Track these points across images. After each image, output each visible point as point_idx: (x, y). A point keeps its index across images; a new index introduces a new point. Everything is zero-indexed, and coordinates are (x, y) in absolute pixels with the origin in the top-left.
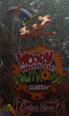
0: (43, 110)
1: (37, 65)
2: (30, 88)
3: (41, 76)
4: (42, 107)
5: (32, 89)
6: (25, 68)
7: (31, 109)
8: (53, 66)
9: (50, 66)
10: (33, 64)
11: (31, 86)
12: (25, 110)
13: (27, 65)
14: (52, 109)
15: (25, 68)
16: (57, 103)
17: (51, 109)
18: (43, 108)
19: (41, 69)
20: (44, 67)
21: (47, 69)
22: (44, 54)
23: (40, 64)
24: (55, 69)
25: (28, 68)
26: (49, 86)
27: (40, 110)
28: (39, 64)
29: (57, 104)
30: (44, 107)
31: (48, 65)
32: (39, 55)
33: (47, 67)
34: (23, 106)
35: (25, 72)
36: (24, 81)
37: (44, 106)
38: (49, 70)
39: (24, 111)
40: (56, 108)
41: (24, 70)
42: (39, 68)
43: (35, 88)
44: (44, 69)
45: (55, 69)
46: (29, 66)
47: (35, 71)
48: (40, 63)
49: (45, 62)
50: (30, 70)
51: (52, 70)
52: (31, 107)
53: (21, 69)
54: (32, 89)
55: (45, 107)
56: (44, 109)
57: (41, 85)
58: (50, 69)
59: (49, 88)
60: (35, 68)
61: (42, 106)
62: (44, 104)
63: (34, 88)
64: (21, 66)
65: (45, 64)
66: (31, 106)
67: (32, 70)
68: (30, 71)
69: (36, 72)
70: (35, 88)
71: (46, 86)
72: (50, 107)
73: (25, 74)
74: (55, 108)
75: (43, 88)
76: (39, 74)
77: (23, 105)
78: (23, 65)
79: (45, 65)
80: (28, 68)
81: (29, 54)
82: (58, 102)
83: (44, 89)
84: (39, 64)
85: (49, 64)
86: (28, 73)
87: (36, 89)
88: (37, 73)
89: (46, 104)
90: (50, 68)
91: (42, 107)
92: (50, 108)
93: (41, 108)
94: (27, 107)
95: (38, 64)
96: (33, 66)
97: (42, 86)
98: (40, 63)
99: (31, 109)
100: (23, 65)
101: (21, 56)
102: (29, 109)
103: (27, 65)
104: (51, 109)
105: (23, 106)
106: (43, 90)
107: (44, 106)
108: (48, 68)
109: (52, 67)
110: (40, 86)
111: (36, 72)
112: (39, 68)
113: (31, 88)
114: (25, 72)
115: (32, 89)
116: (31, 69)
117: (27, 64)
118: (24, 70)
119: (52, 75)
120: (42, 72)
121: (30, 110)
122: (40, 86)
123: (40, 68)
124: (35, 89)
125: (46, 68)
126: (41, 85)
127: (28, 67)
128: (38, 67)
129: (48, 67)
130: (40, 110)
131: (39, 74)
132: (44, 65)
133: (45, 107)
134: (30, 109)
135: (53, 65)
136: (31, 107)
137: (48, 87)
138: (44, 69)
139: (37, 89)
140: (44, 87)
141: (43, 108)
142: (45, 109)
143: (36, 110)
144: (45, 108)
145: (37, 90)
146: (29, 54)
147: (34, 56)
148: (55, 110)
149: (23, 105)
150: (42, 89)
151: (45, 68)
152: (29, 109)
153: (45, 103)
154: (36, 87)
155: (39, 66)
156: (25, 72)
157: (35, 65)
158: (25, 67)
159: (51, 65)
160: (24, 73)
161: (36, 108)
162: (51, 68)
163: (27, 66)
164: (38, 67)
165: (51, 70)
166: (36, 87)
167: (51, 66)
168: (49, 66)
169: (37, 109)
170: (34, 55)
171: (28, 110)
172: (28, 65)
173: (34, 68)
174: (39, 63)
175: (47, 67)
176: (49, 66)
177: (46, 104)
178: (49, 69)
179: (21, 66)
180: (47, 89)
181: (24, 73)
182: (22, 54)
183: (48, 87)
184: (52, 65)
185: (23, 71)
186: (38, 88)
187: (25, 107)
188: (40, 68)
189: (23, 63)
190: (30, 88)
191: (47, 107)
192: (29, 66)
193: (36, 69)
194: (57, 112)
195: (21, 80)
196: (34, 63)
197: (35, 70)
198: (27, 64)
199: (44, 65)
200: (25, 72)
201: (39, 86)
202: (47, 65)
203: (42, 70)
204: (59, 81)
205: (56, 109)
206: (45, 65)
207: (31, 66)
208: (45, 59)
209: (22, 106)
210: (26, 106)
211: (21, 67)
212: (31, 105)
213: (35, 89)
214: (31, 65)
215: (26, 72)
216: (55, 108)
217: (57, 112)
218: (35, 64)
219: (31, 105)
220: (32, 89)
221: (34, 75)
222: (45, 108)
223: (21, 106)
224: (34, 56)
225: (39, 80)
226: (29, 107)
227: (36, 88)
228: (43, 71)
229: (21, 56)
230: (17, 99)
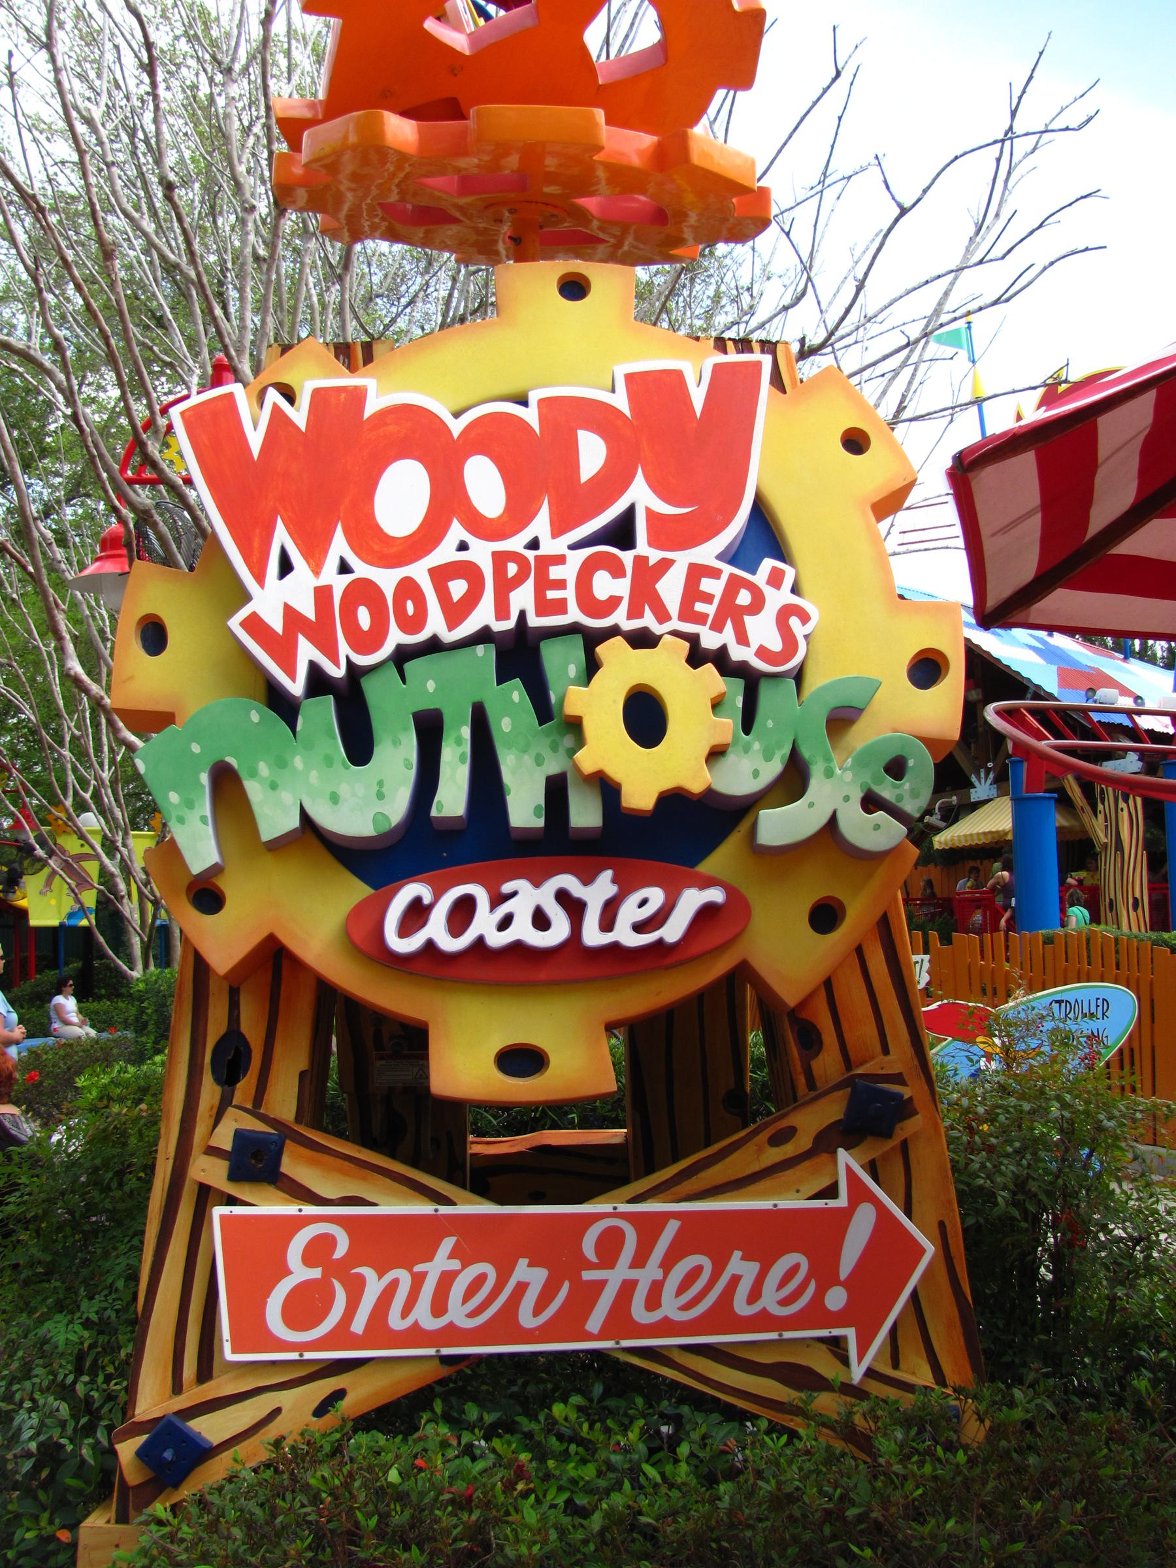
0: (640, 1314)
1: (500, 559)
2: (406, 929)
3: (575, 726)
4: (615, 1277)
5: (436, 929)
6: (308, 610)
7: (439, 1307)
8: (760, 577)
9: (715, 573)
10: (445, 553)
11: (413, 890)
12: (358, 1325)
13: (353, 560)
14: (769, 1301)
15: (308, 610)
16: (842, 1201)
17: (755, 1294)
18: (628, 1287)
19: (574, 629)
20: (622, 587)
21: (675, 624)
22: (620, 401)
23: (549, 547)
24: (805, 618)
25: (364, 618)
26: (716, 895)
27: (594, 1323)
28: (534, 544)
29: (845, 1216)
30: (651, 1271)
31: (683, 559)
32: (531, 415)
33: (671, 589)
34: (316, 1273)
35: (318, 682)
36: (305, 816)
37: (639, 1261)
38: (710, 640)
39: (341, 1336)
40: (835, 1281)
41: (306, 652)
42: (544, 607)
43: (484, 924)
44: (619, 617)
45: (805, 618)
46: (387, 580)
47: (480, 650)
48: (558, 530)
49: (630, 512)
50: (396, 637)
51: (742, 638)
52: (447, 1279)
53: (255, 625)
54: (430, 945)
55: (667, 1264)
56: (653, 1301)
57: (587, 880)
58: (718, 627)
59: (706, 913)
60: (483, 616)
61: (608, 1258)
62: (649, 1227)
63: (463, 912)
64: (260, 579)
65: (642, 546)
66: (442, 1261)
67: (434, 646)
68: (402, 656)
69: (502, 677)
70: (484, 924)
71: (656, 896)
72: (740, 1266)
73: (326, 706)
74: (824, 1273)
75: (607, 924)
76: (544, 710)
77: (309, 1259)
78: (286, 567)
79: (640, 561)
80: (364, 618)
81: (372, 407)
82: (859, 1194)
83: (625, 935)
84: (534, 544)
85: (707, 553)
86: (372, 688)
87: (497, 940)
88: (516, 692)
89: (673, 1226)
90: (710, 609)
91: (615, 1277)
92: (735, 1280)
93: (601, 1284)
94: (374, 1286)
95: (516, 543)
96: (441, 576)
97: (603, 887)
98: (558, 530)
99: (439, 1307)
100: (286, 567)
101: (255, 440)
102: (406, 1312)
103: (344, 568)
104: (755, 1294)
105: (316, 1273)
106: (615, 947)
107: (639, 1261)
108: (687, 613)
109: (744, 598)
110: (563, 897)
111: (502, 677)
112: (540, 613)
113: (417, 914)
114: (314, 668)
115: (436, 929)
116: (413, 624)
117: (339, 546)
118: (306, 652)
119: (748, 723)
120: (592, 666)
121: (430, 1323)
122: (563, 897)
123: (560, 607)
124: (480, 941)
125: (662, 615)
126: (587, 880)
127: (364, 592)
128: (523, 598)
129: (692, 593)
130: (594, 1323)
131: (544, 710)
132: (627, 557)
133: (667, 1264)
134: (422, 1314)
135: (768, 564)
136: (447, 1279)
137: (692, 900)
138: (614, 631)
139: (523, 931)
140: (629, 912)
141: (628, 1287)
142: (670, 1307)
143: (527, 1318)
144: (656, 1289)
145: (518, 947)
146: (372, 407)
147: (456, 427)
148: (815, 1314)
149: (318, 1251)
150: (592, 936)
151: (635, 612)
152: (406, 1312)
153: (662, 1219)
154: (498, 900)
155: (544, 584)
156: (318, 682)
157: (470, 572)
158: (323, 595)
159: (732, 556)
160: (296, 687)
161: (522, 1287)
162: (730, 613)
163: (340, 584)
164: (523, 598)
165: (727, 636)
166: (498, 900)
167: (734, 584)
168: (696, 572)
169: (538, 1310)
170: (457, 415)
171: (396, 1322)
172: (362, 569)
173: (455, 613)
174: (540, 525)
175: (671, 589)
176: (696, 572)
177: (673, 1226)
178: (701, 619)
179: (260, 579)
180: (673, 931)
181: (296, 687)
182: (276, 408)
183: (692, 900)
184: (753, 571)
185: (289, 666)
186: (541, 921)
187: (356, 1289)
188: (560, 607)
189: (281, 536)
190: (406, 929)
191: (696, 1271)
192: (387, 580)
193: (499, 626)
194: (850, 1333)
195: (254, 789)
196: (457, 531)
197: (484, 636)
198: (339, 546)
199: (617, 570)
200: (314, 668)
201: (545, 896)
202: (666, 564)
203: (592, 639)
204: (871, 802)
205: (836, 1299)
206: (640, 561)
207: (408, 588)
208: (639, 478)
209: (300, 1273)
210: (368, 1272)
211: (247, 598)
212: (448, 1243)
213: (480, 941)
214: (419, 571)
215: (337, 672)
216: (824, 1273)
217: (850, 1333)
218: (481, 553)
219: (448, 1243)
220: (430, 945)
221: (466, 732)
222: (656, 1289)
223: (288, 1272)
224: (456, 427)
225: (539, 797)
226: (418, 1280)
227: (505, 923)
228: (612, 651)
229: (255, 440)
230: (213, 1151)
